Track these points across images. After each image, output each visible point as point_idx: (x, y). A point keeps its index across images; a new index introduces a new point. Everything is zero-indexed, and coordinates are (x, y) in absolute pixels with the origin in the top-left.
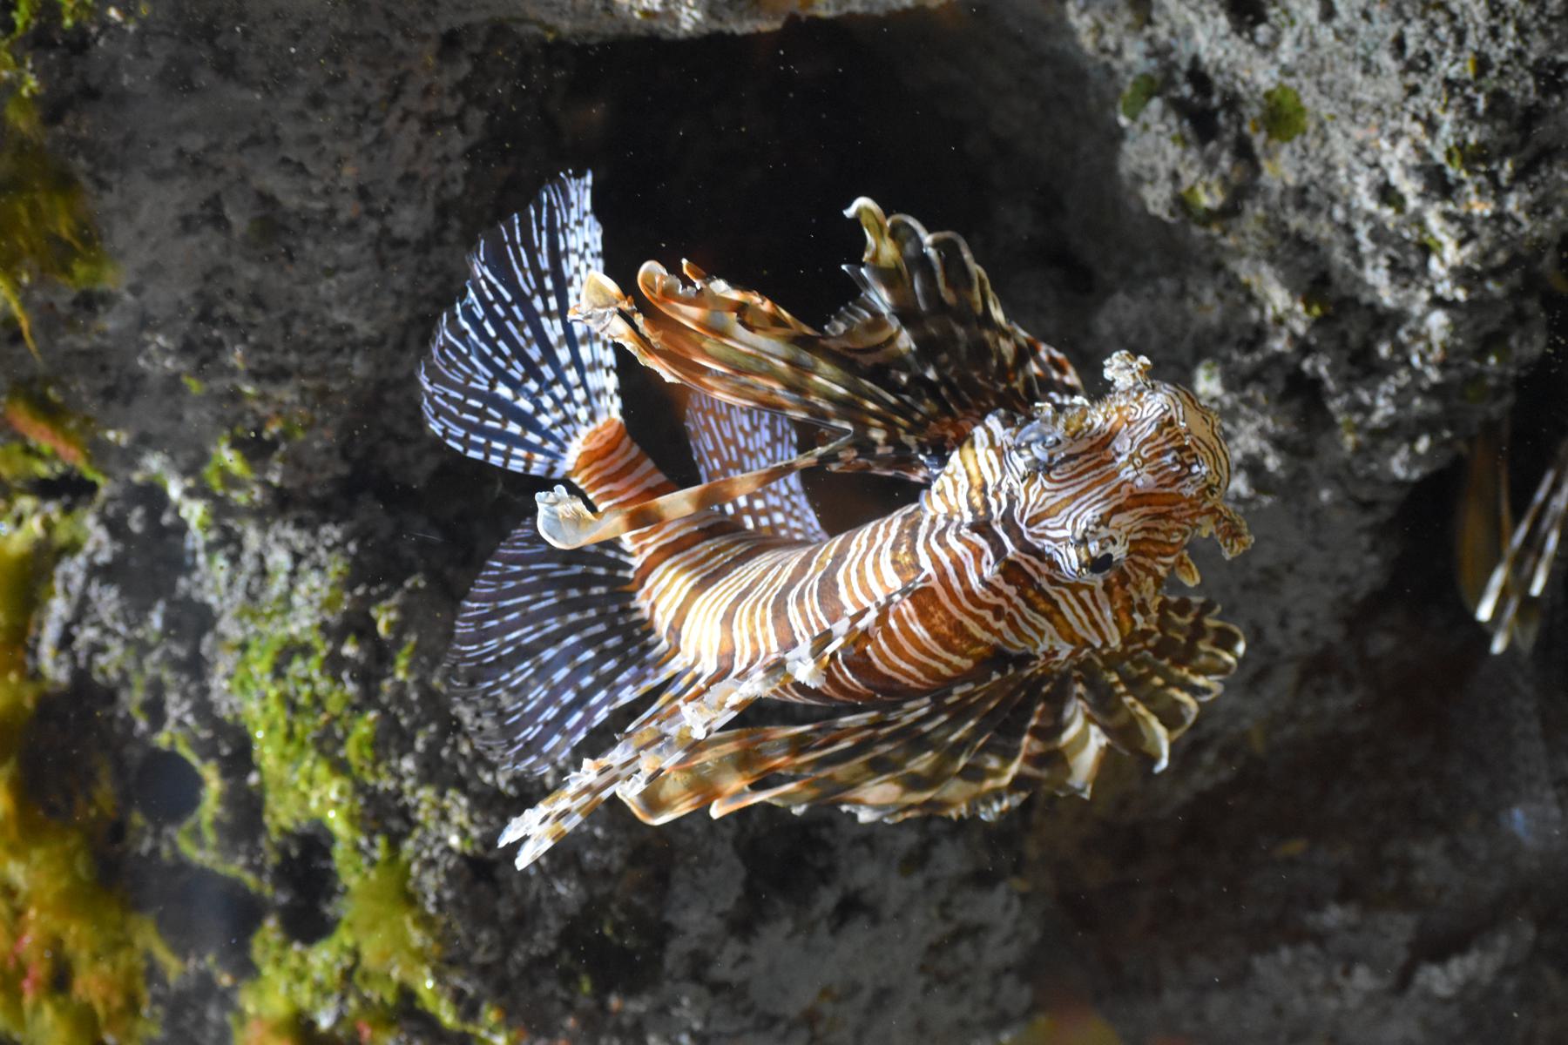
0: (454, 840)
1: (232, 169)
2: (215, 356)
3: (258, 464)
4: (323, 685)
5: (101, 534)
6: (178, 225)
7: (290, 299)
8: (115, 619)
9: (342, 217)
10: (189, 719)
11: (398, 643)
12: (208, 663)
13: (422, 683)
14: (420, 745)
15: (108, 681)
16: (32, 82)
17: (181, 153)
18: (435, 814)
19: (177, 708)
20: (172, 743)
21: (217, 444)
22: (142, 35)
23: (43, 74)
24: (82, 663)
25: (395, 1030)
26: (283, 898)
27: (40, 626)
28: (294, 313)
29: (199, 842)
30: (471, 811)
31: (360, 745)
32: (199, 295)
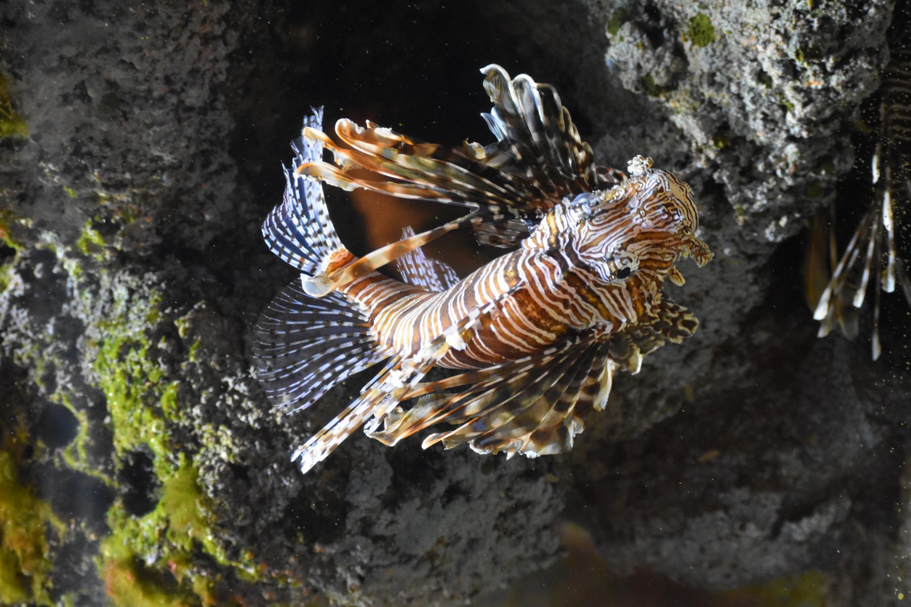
0: (224, 455)
1: (91, 67)
2: (83, 175)
3: (109, 237)
4: (147, 366)
5: (18, 279)
6: (61, 99)
7: (126, 142)
8: (26, 329)
9: (156, 94)
10: (70, 386)
11: (191, 341)
12: (81, 354)
13: (204, 364)
14: (203, 401)
15: (22, 364)
17: (62, 58)
18: (213, 439)
19: (62, 379)
20: (60, 400)
21: (84, 227)
24: (7, 354)
25: (190, 565)
26: (125, 489)
28: (129, 150)
29: (76, 457)
30: (233, 437)
31: (169, 401)
32: (73, 140)
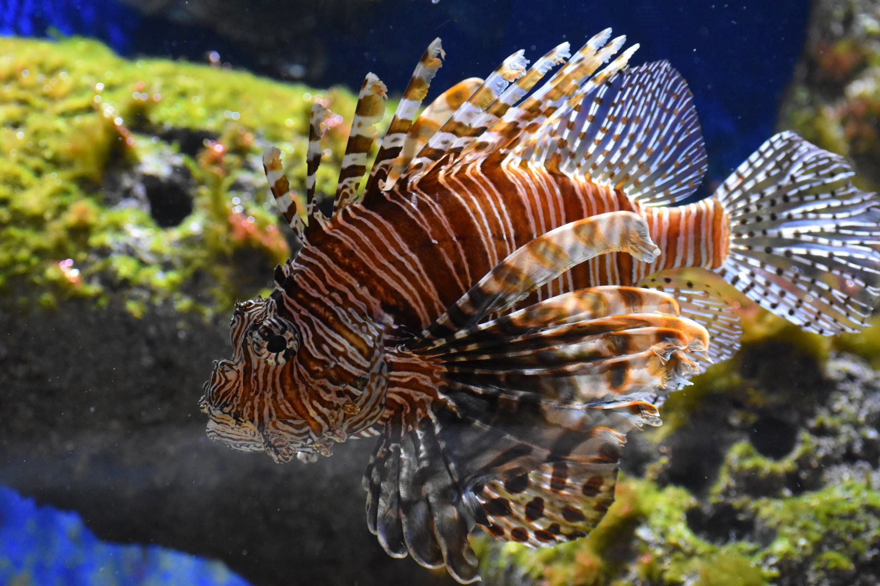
19: (827, 444)
20: (803, 442)
26: (707, 509)
27: (854, 362)
29: (738, 454)
31: (835, 560)
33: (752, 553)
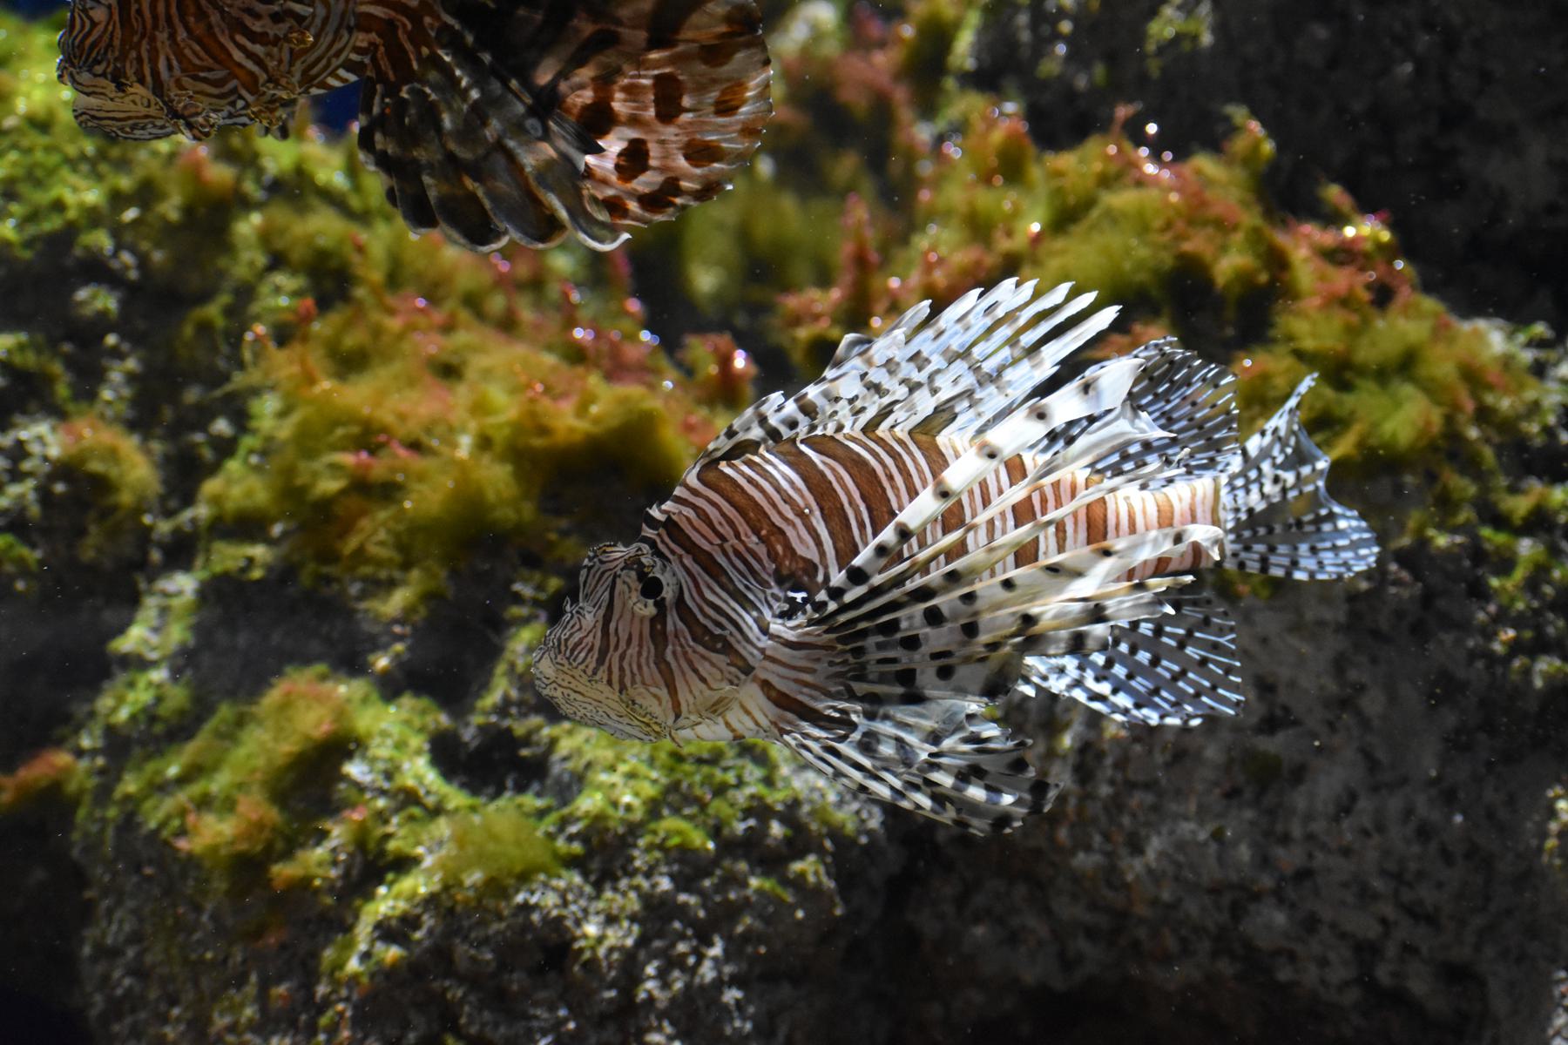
0: (591, 929)
4: (741, 797)
9: (1280, 852)
11: (785, 882)
13: (745, 905)
14: (683, 897)
16: (1442, 541)
17: (1361, 688)
18: (615, 912)
22: (1491, 658)
23: (1447, 554)
26: (468, 735)
30: (621, 949)
31: (679, 833)
33: (541, 814)
